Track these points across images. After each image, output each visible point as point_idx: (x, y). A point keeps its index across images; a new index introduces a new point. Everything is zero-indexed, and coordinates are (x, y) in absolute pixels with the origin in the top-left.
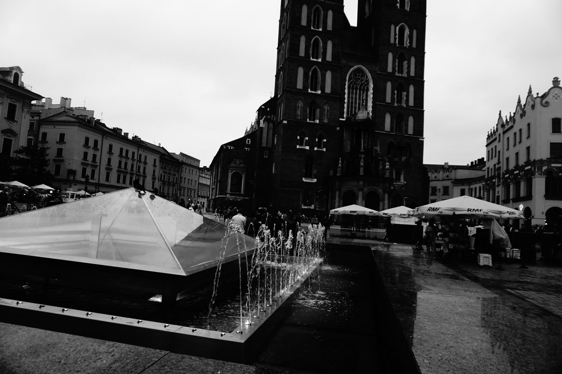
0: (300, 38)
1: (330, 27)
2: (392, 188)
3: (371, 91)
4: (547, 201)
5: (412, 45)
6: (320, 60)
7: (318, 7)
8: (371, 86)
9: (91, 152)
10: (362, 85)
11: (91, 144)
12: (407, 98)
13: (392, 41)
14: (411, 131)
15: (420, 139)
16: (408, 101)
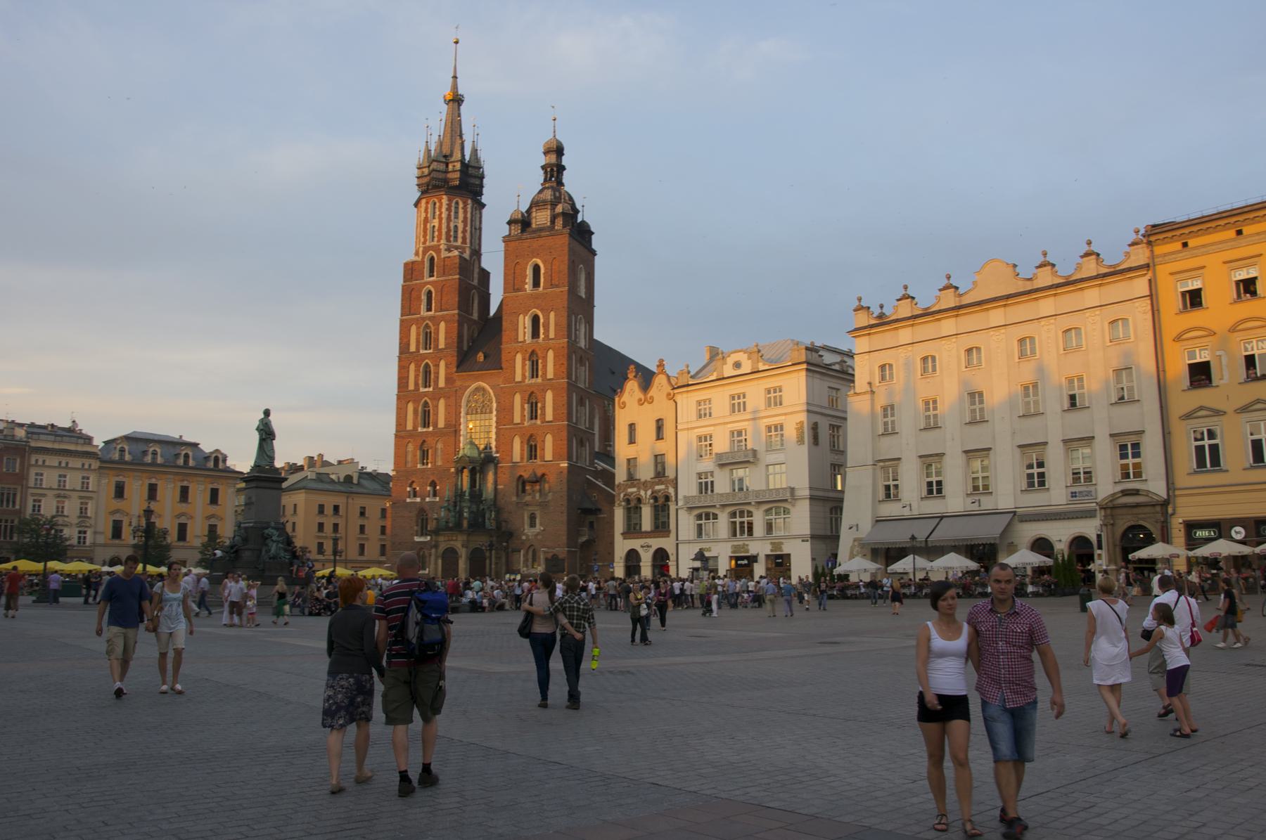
0: (409, 367)
1: (442, 345)
2: (524, 538)
3: (495, 413)
4: (625, 541)
5: (548, 336)
6: (431, 389)
7: (427, 324)
8: (495, 405)
9: (329, 523)
10: (483, 406)
11: (329, 510)
12: (542, 412)
13: (521, 339)
14: (549, 456)
15: (562, 465)
16: (545, 414)
